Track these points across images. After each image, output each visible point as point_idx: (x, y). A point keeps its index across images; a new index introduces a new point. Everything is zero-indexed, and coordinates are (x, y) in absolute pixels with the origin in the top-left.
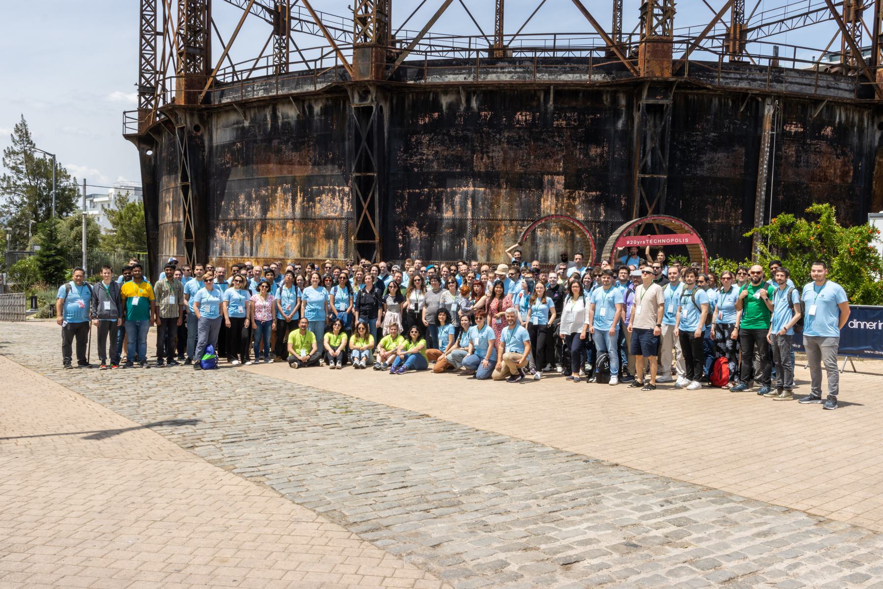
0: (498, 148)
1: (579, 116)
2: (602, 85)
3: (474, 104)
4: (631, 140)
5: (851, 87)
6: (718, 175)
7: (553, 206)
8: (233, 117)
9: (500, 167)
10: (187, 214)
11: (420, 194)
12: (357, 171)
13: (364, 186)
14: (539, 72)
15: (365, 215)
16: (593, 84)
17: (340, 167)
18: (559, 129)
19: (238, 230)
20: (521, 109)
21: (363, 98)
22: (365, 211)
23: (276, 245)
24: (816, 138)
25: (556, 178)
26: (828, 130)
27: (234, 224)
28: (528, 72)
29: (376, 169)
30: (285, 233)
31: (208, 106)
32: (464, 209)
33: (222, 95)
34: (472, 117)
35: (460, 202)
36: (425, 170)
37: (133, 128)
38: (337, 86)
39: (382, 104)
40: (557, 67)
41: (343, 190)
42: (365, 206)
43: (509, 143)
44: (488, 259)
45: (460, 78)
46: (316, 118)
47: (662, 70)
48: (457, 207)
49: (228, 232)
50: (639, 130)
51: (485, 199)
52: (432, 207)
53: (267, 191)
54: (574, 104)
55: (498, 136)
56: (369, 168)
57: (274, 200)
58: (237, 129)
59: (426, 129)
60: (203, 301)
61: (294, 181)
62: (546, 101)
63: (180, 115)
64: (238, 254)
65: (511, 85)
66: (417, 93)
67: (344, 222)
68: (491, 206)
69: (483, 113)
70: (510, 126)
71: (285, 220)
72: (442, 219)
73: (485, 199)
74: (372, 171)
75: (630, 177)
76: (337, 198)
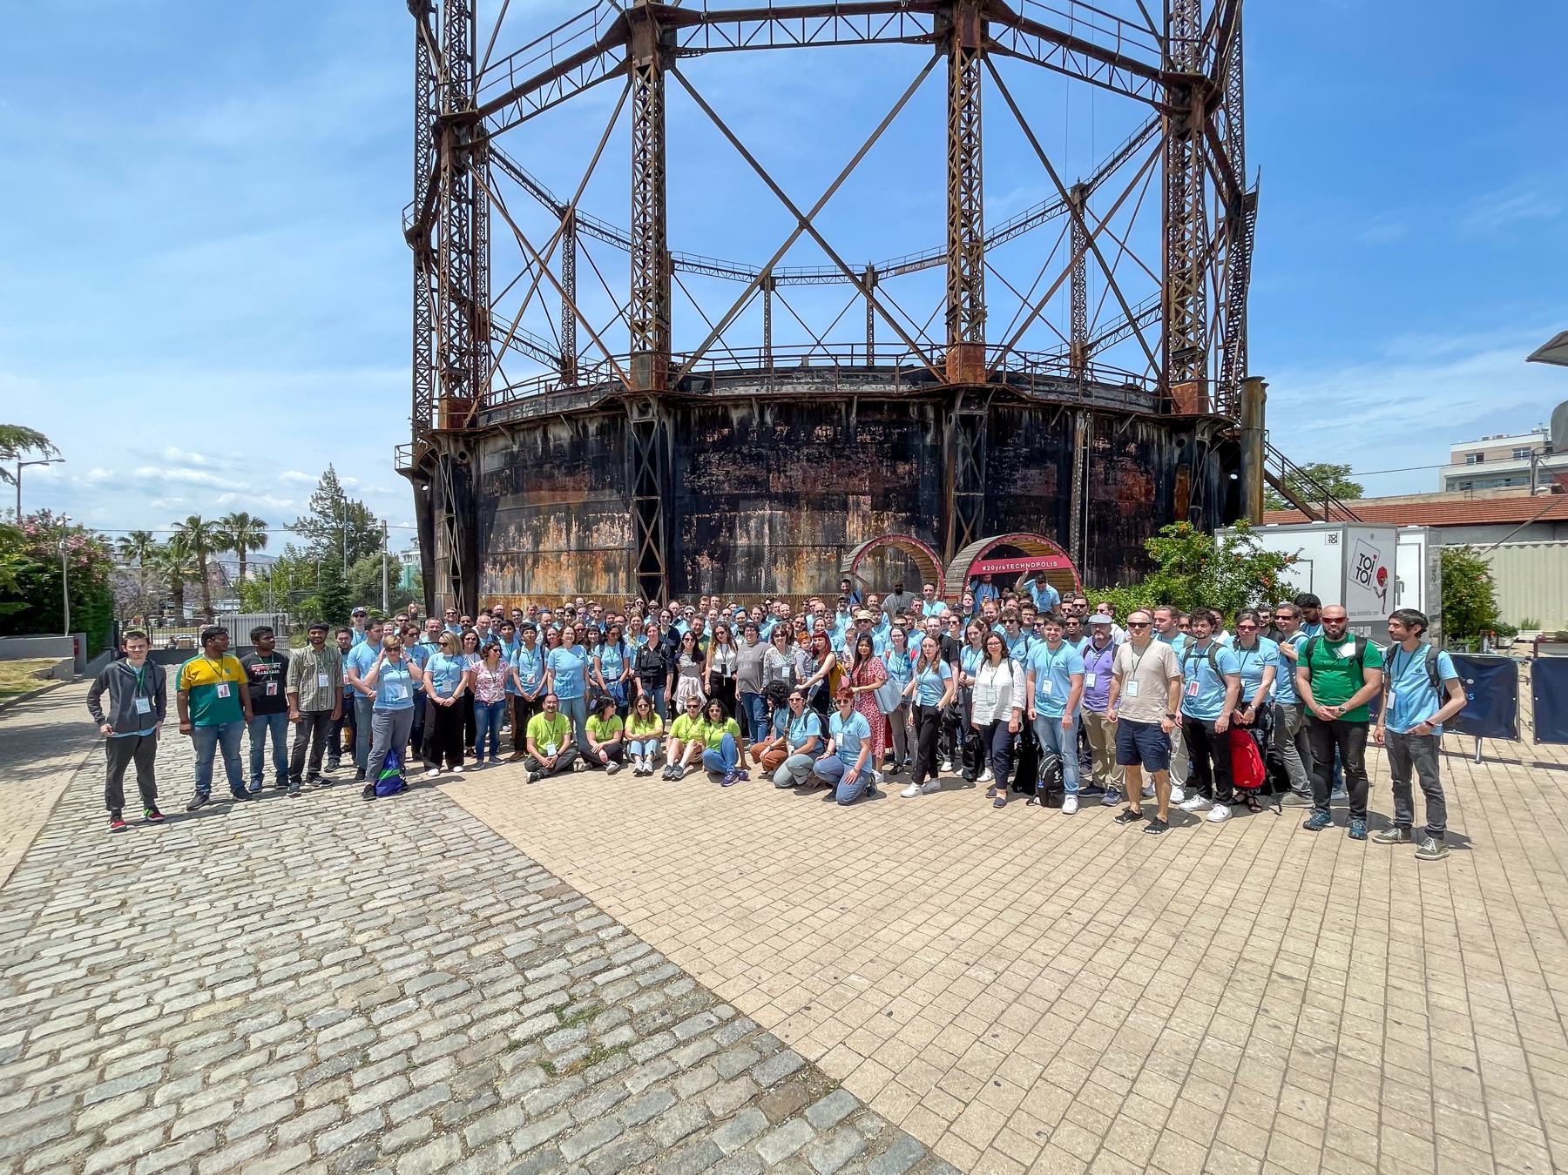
1: (884, 430)
3: (768, 419)
4: (941, 455)
5: (1151, 404)
6: (1032, 494)
8: (501, 442)
9: (799, 487)
11: (710, 519)
12: (639, 493)
13: (647, 510)
16: (900, 395)
17: (619, 492)
18: (864, 444)
21: (642, 413)
22: (649, 540)
24: (1122, 455)
26: (1132, 447)
27: (504, 558)
28: (826, 382)
29: (659, 491)
31: (472, 429)
32: (760, 535)
34: (766, 433)
37: (408, 462)
38: (612, 399)
40: (857, 377)
42: (648, 534)
43: (808, 460)
45: (752, 390)
48: (753, 533)
50: (950, 446)
53: (538, 520)
54: (878, 417)
56: (652, 491)
57: (547, 531)
59: (719, 446)
62: (848, 415)
64: (508, 591)
65: (812, 396)
66: (704, 408)
67: (625, 553)
70: (809, 442)
72: (736, 547)
73: (784, 523)
74: (655, 494)
76: (616, 526)
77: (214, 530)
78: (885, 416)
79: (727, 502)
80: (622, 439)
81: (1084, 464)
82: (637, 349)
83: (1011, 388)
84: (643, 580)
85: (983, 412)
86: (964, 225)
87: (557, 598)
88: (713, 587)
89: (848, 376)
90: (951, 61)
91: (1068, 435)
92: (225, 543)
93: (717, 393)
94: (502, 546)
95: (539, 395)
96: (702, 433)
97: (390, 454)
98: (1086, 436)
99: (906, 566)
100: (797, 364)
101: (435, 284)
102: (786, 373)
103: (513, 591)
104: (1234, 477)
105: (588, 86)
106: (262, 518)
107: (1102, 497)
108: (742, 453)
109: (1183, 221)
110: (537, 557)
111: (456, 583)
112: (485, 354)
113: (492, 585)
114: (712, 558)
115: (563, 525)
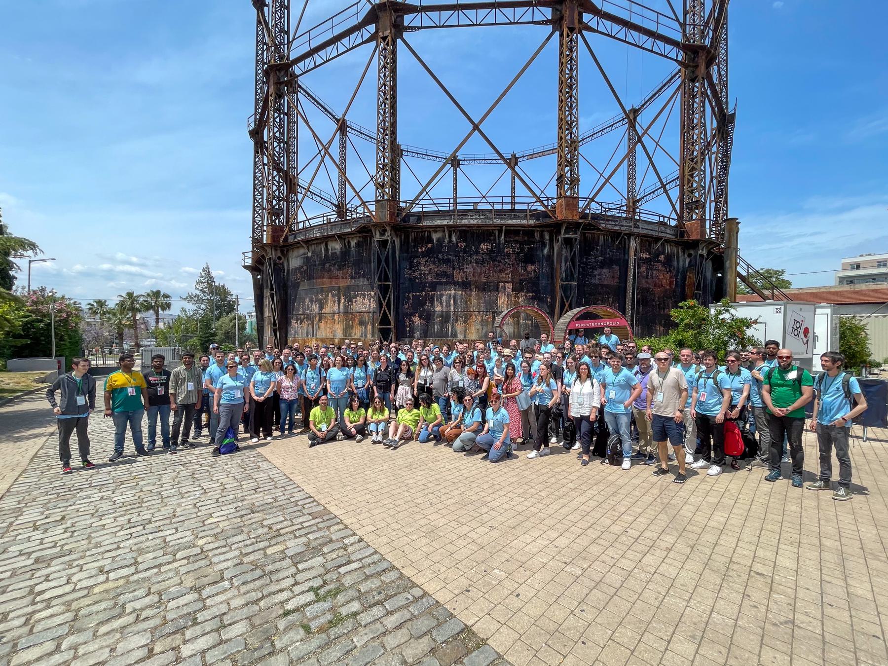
0: (470, 265)
3: (454, 239)
4: (553, 261)
7: (506, 303)
8: (302, 251)
9: (471, 278)
11: (420, 296)
12: (379, 280)
13: (384, 290)
15: (385, 309)
16: (530, 226)
17: (368, 280)
18: (508, 254)
19: (305, 320)
20: (484, 242)
21: (382, 234)
22: (384, 307)
23: (328, 330)
25: (507, 285)
26: (662, 257)
29: (391, 280)
32: (448, 305)
34: (453, 247)
36: (423, 281)
37: (249, 262)
40: (505, 215)
42: (384, 304)
43: (476, 263)
44: (465, 337)
45: (445, 222)
47: (573, 216)
48: (444, 304)
49: (299, 322)
50: (557, 255)
52: (428, 304)
53: (322, 295)
54: (517, 238)
56: (387, 279)
57: (327, 302)
59: (424, 255)
60: (224, 386)
62: (499, 237)
64: (305, 336)
65: (478, 226)
66: (417, 232)
67: (371, 315)
68: (466, 303)
69: (460, 244)
70: (477, 253)
71: (334, 313)
72: (434, 312)
74: (388, 281)
75: (553, 284)
76: (366, 299)
77: (141, 299)
78: (521, 238)
80: (370, 249)
81: (635, 267)
82: (379, 198)
83: (593, 222)
84: (381, 330)
85: (577, 236)
86: (567, 129)
87: (332, 339)
88: (421, 334)
89: (499, 215)
90: (561, 35)
91: (625, 250)
92: (147, 307)
93: (425, 224)
94: (301, 310)
95: (324, 224)
96: (415, 246)
97: (239, 258)
98: (636, 250)
99: (532, 323)
100: (472, 208)
101: (266, 161)
102: (465, 213)
104: (720, 275)
105: (353, 48)
106: (168, 292)
107: (645, 286)
108: (438, 259)
109: (693, 128)
110: (321, 316)
111: (275, 331)
112: (294, 202)
113: (295, 332)
114: (420, 317)
115: (336, 299)
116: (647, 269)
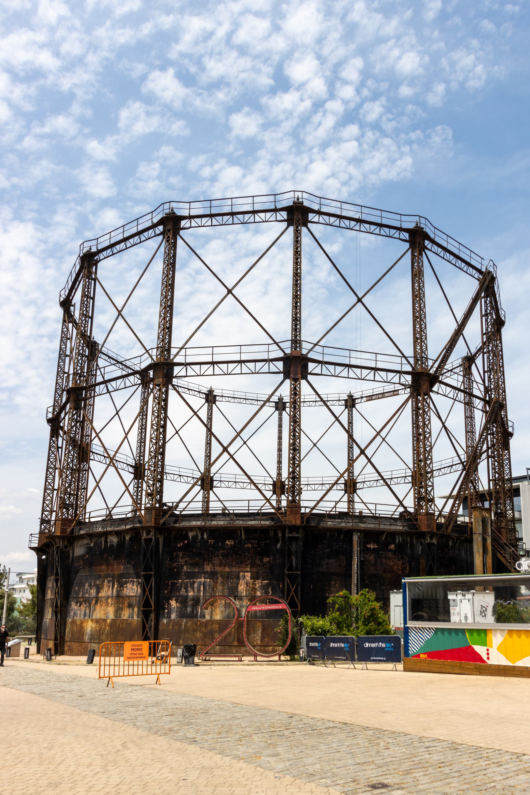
2: (268, 526)
3: (205, 536)
10: (57, 595)
13: (147, 579)
14: (238, 520)
18: (248, 548)
20: (228, 539)
21: (148, 533)
22: (147, 592)
28: (231, 520)
29: (153, 570)
30: (107, 605)
32: (199, 590)
33: (80, 529)
35: (197, 587)
39: (158, 536)
41: (138, 581)
42: (147, 590)
43: (222, 556)
45: (199, 523)
46: (126, 543)
48: (196, 590)
51: (210, 585)
52: (183, 590)
53: (99, 581)
55: (217, 553)
58: (87, 548)
61: (113, 577)
63: (57, 541)
67: (138, 598)
69: (210, 541)
71: (108, 597)
72: (188, 596)
73: (210, 585)
74: (151, 571)
79: (185, 576)
87: (105, 620)
88: (176, 615)
94: (81, 594)
103: (85, 617)
115: (111, 584)
116: (375, 558)
